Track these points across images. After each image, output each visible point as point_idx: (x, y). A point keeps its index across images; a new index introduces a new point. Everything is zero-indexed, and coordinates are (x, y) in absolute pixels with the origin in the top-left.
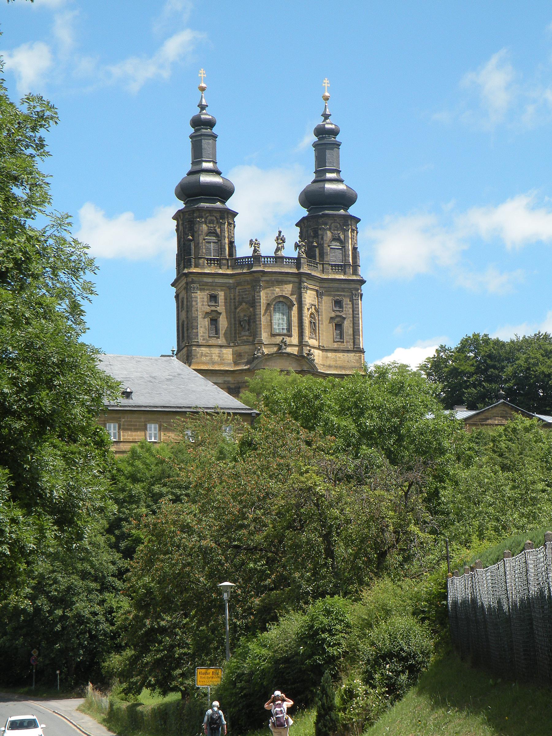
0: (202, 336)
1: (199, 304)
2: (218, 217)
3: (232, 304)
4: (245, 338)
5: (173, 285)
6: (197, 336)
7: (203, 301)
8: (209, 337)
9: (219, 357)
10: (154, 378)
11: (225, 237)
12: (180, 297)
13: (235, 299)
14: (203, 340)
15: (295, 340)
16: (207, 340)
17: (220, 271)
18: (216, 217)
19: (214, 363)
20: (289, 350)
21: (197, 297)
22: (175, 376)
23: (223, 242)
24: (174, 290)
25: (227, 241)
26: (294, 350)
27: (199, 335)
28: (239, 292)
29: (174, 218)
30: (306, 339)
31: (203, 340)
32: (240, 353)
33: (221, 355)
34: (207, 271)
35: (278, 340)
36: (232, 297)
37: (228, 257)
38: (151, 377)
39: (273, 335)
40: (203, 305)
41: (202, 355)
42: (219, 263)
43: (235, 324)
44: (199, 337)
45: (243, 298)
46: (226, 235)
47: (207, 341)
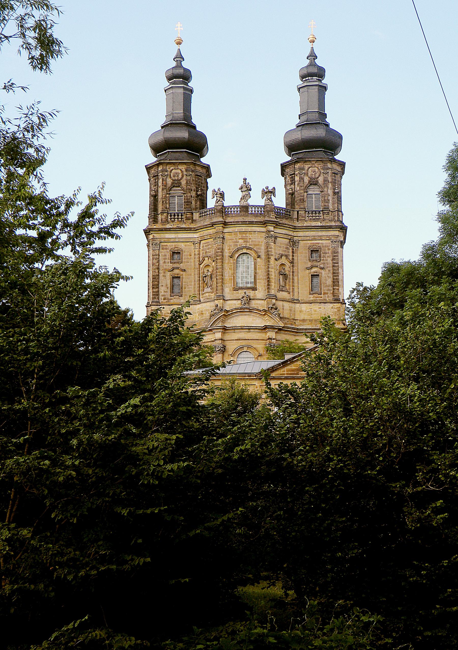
0: (163, 296)
2: (184, 170)
4: (207, 294)
7: (165, 259)
13: (199, 254)
14: (164, 299)
16: (168, 299)
17: (184, 226)
18: (180, 170)
27: (161, 294)
28: (203, 247)
31: (164, 299)
36: (197, 253)
40: (165, 262)
44: (160, 297)
45: (206, 252)
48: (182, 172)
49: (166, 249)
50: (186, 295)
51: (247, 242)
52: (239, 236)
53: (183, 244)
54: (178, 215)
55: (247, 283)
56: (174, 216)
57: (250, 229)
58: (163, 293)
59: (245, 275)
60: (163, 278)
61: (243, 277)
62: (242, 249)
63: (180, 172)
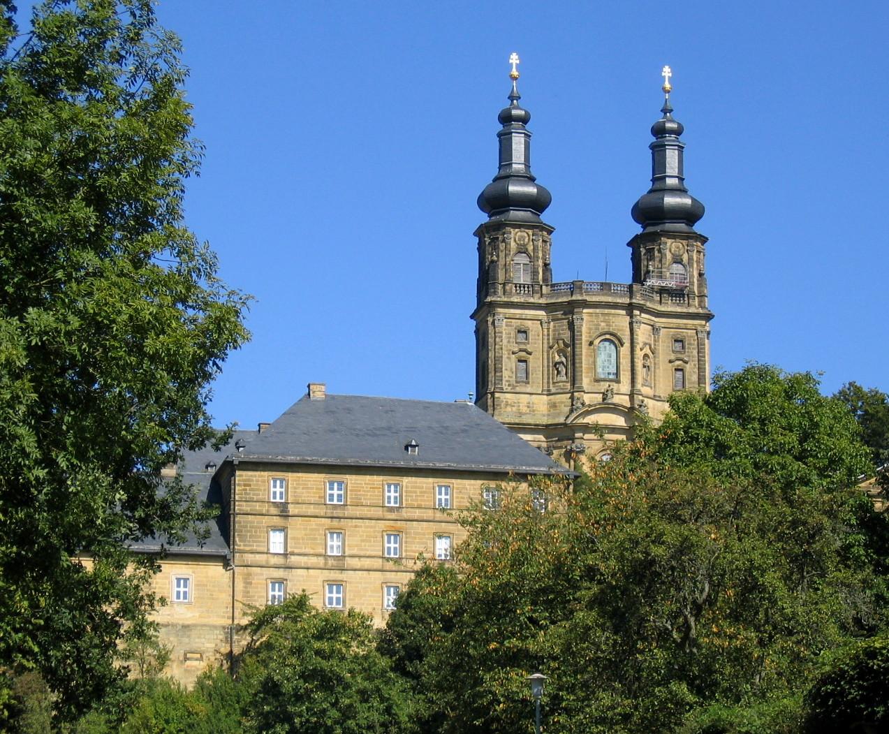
0: (507, 381)
1: (505, 341)
3: (545, 341)
5: (472, 317)
6: (502, 380)
8: (517, 382)
9: (528, 407)
10: (447, 428)
11: (538, 257)
12: (481, 332)
14: (509, 385)
15: (625, 387)
19: (521, 414)
20: (617, 399)
21: (501, 333)
22: (472, 427)
23: (536, 263)
24: (474, 323)
25: (540, 263)
26: (624, 401)
29: (475, 234)
30: (639, 386)
31: (509, 385)
32: (555, 403)
33: (531, 405)
34: (515, 299)
35: (604, 386)
37: (541, 283)
38: (443, 427)
39: (597, 381)
40: (509, 342)
41: (507, 404)
42: (533, 288)
43: (548, 366)
44: (504, 382)
45: (559, 334)
46: (540, 255)
47: (514, 387)
48: (529, 235)
49: (511, 326)
50: (533, 382)
51: (610, 326)
52: (601, 318)
53: (530, 322)
54: (524, 287)
55: (609, 374)
56: (520, 287)
57: (613, 311)
58: (507, 378)
59: (606, 364)
60: (507, 360)
61: (604, 367)
62: (605, 334)
63: (526, 235)
